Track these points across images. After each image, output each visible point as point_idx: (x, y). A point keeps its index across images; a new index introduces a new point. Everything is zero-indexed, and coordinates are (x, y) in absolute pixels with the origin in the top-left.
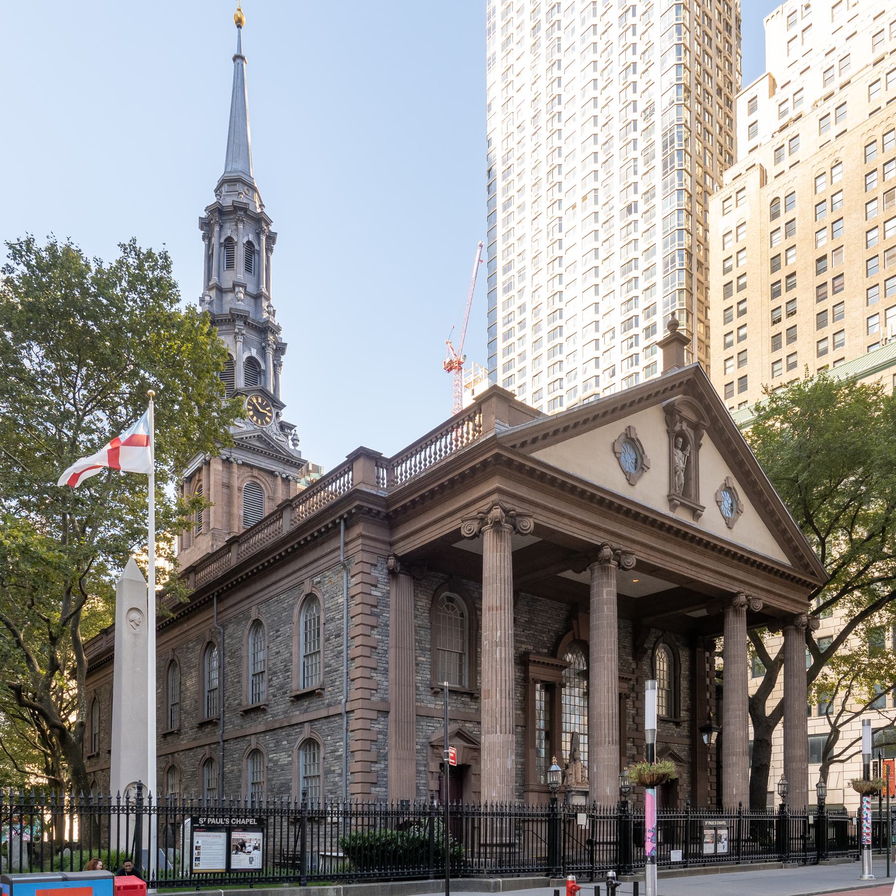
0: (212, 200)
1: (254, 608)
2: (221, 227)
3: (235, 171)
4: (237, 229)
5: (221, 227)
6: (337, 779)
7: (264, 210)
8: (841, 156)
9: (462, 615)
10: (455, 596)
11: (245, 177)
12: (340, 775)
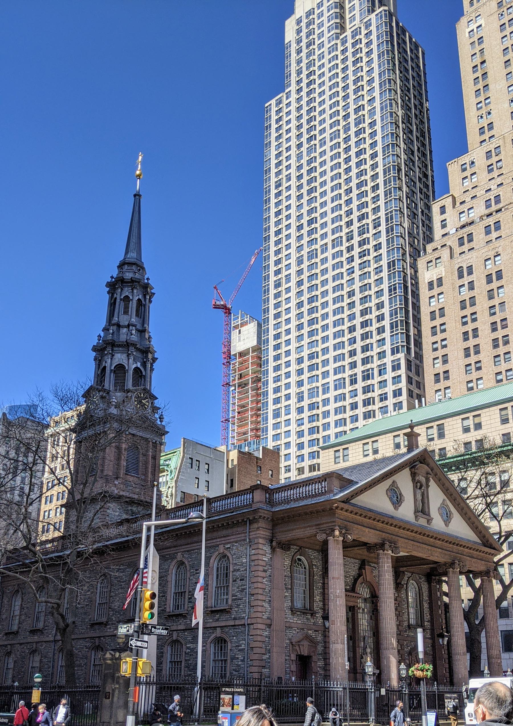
0: (115, 273)
1: (179, 554)
2: (122, 289)
3: (132, 258)
4: (133, 292)
5: (122, 289)
6: (240, 663)
7: (149, 282)
8: (500, 250)
9: (305, 568)
10: (302, 558)
11: (139, 263)
12: (242, 661)
